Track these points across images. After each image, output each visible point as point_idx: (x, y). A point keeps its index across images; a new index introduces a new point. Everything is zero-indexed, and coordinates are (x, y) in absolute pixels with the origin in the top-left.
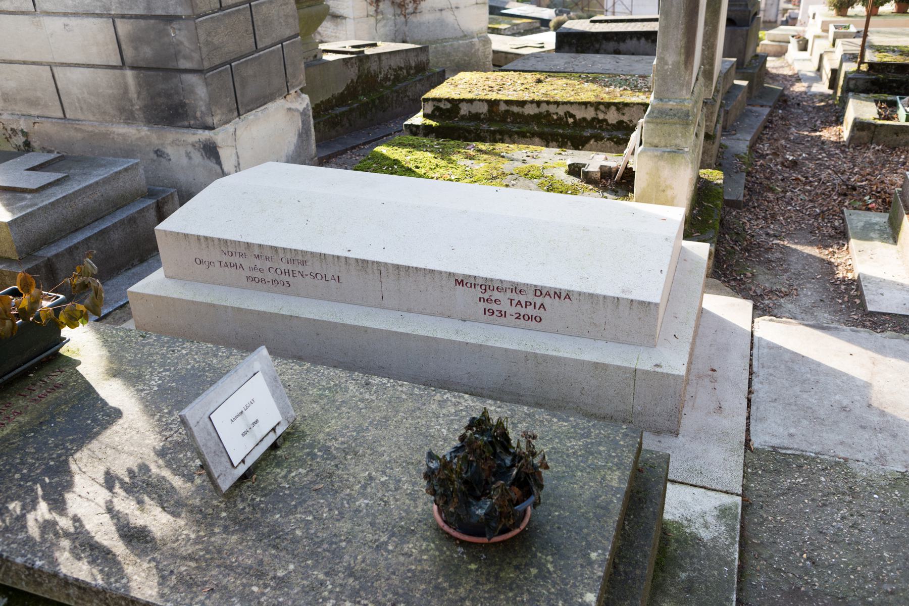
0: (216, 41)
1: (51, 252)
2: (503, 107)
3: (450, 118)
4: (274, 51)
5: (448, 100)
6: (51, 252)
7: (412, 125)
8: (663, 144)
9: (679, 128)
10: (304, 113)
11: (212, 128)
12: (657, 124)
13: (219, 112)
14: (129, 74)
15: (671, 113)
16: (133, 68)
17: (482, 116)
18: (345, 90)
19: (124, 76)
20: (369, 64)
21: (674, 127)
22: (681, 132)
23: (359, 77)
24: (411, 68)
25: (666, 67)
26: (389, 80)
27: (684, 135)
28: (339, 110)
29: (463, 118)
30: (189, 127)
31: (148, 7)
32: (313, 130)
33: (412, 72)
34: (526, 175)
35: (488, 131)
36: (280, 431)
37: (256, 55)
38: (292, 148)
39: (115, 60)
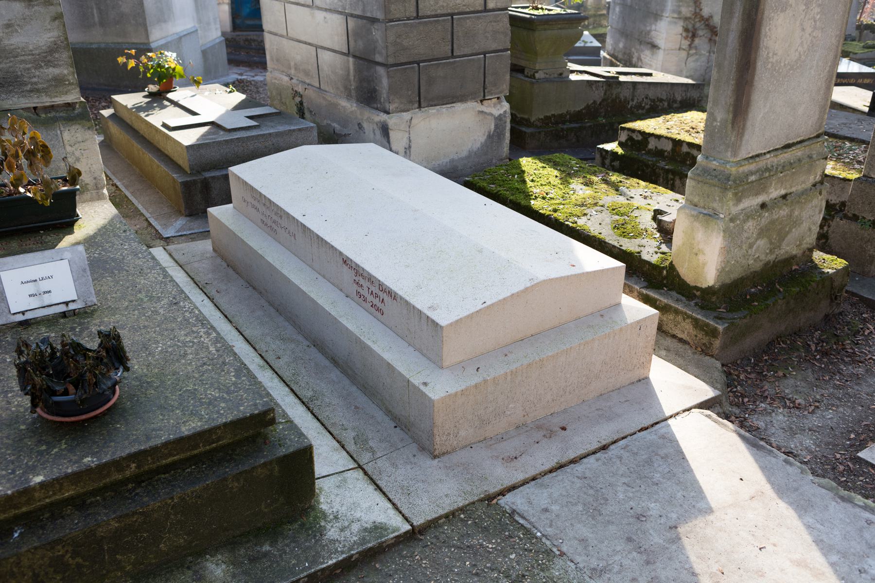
0: (405, 43)
1: (207, 175)
2: (685, 149)
3: (639, 150)
4: (473, 60)
5: (639, 132)
6: (207, 175)
7: (603, 149)
8: (702, 205)
9: (717, 191)
10: (499, 119)
11: (388, 113)
12: (699, 182)
13: (396, 100)
14: (351, 59)
15: (714, 173)
16: (354, 56)
17: (666, 154)
18: (584, 109)
19: (348, 61)
20: (619, 90)
21: (713, 189)
22: (719, 196)
23: (603, 100)
24: (675, 101)
25: (715, 124)
26: (643, 108)
27: (721, 200)
28: (568, 125)
29: (650, 152)
30: (377, 109)
31: (364, 10)
32: (508, 135)
33: (675, 105)
34: (613, 210)
35: (663, 169)
36: (72, 307)
37: (451, 60)
38: (478, 145)
39: (345, 50)
